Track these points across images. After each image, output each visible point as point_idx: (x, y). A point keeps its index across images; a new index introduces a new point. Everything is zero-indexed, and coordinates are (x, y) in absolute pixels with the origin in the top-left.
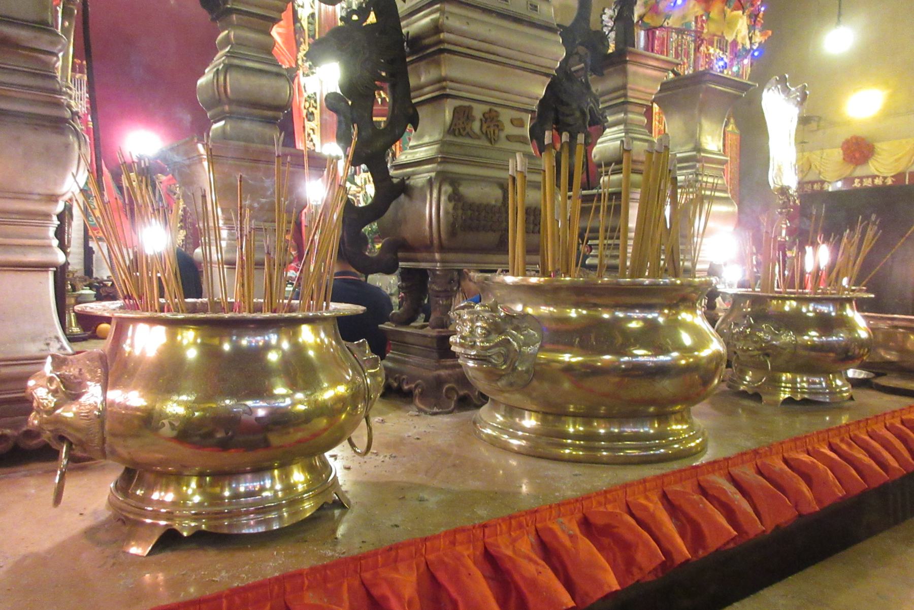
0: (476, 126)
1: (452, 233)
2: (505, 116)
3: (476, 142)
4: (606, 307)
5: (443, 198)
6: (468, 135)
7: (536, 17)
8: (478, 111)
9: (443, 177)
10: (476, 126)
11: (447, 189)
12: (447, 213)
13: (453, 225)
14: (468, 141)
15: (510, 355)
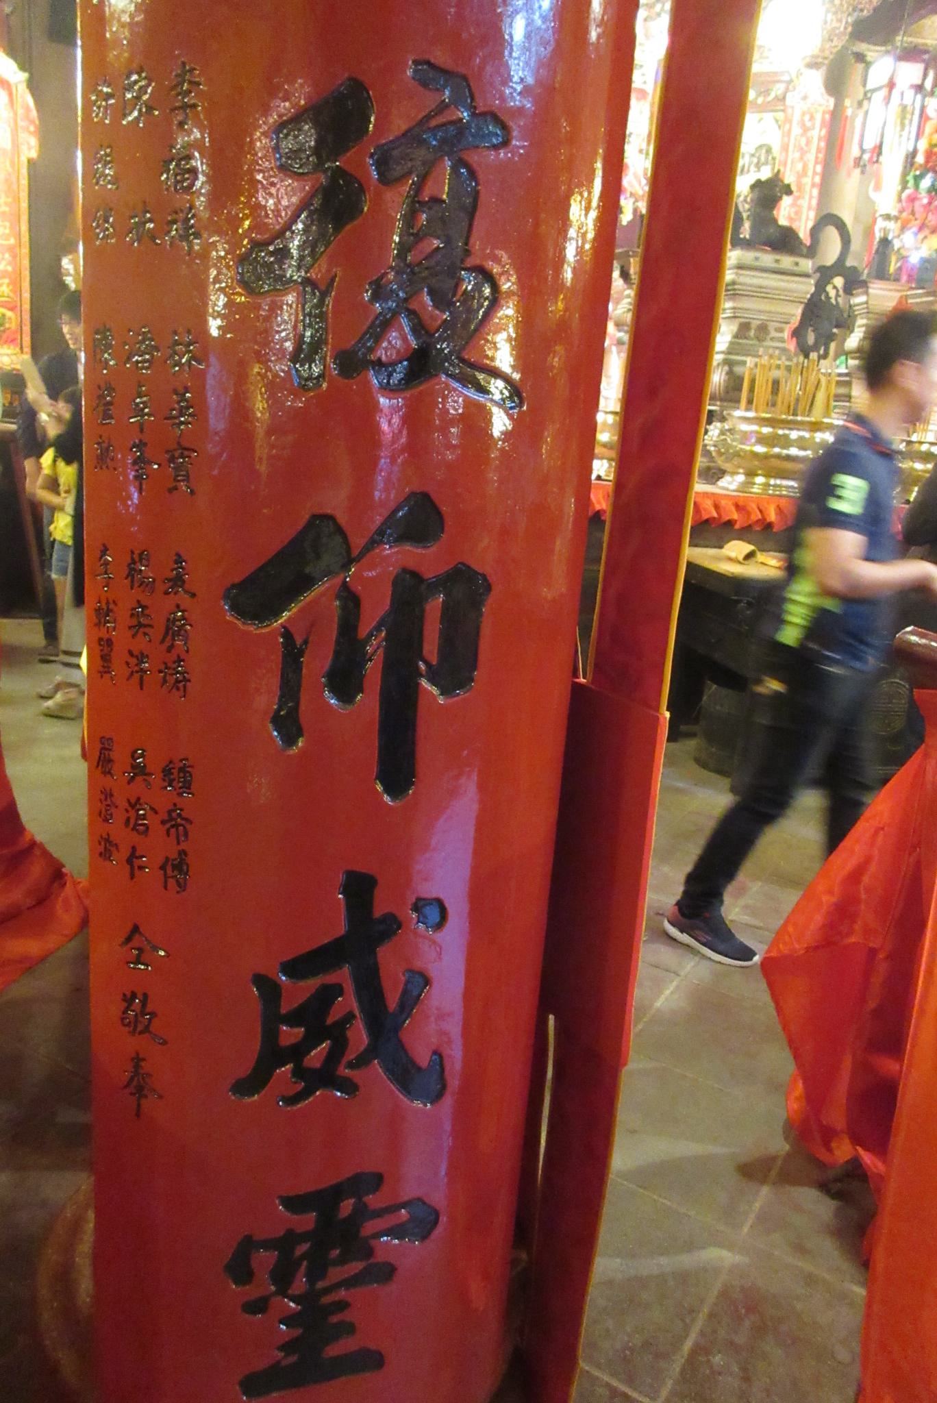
0: (752, 333)
1: (727, 392)
2: (772, 326)
3: (751, 342)
4: (780, 428)
5: (724, 373)
6: (746, 338)
7: (800, 269)
8: (755, 324)
9: (726, 362)
10: (752, 333)
11: (726, 368)
12: (724, 381)
13: (727, 387)
14: (744, 341)
15: (729, 446)
